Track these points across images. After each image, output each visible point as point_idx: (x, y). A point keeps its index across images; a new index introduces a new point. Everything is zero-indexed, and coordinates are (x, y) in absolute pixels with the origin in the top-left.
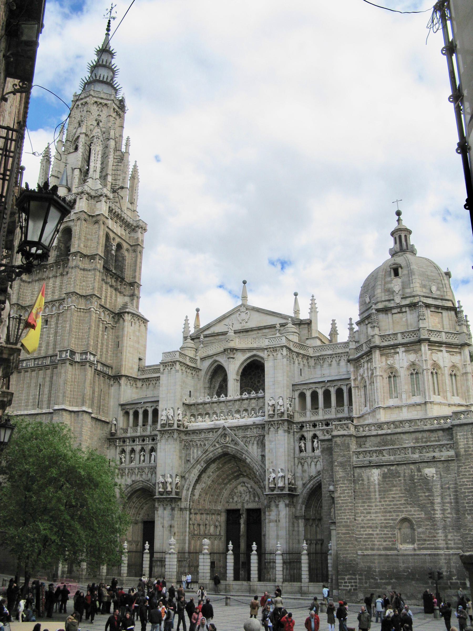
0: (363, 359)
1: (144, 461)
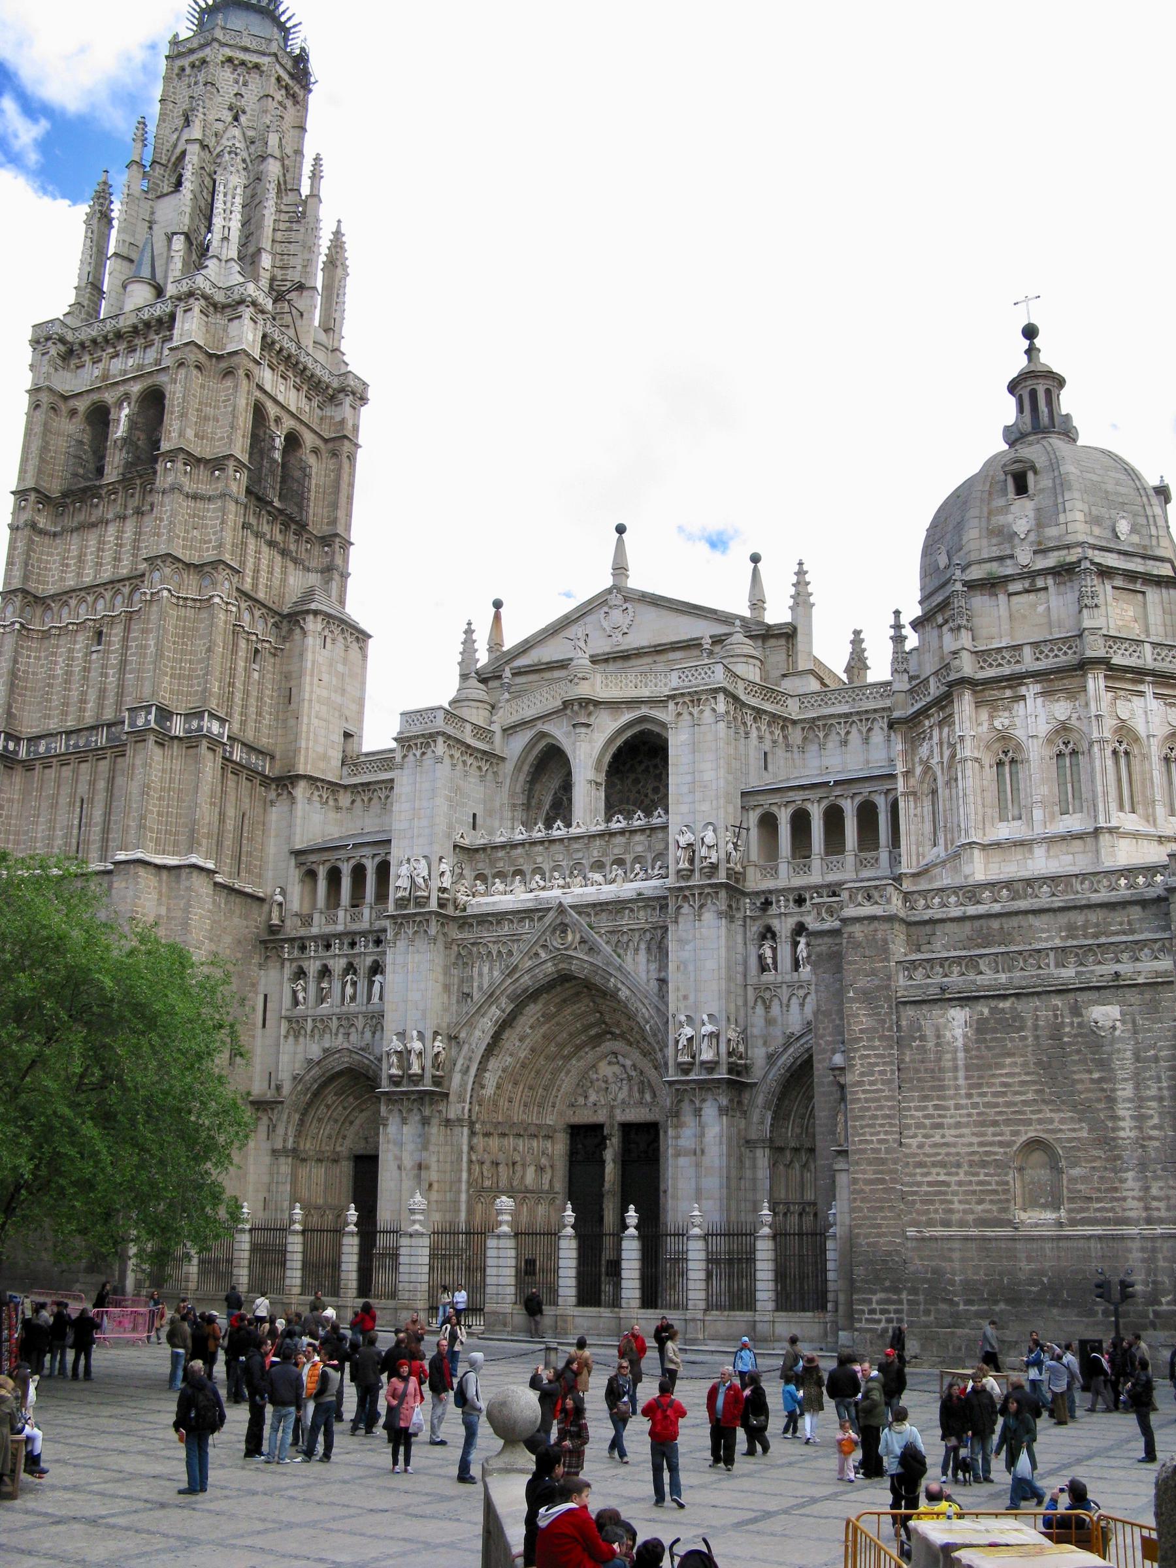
0: (928, 717)
1: (353, 998)
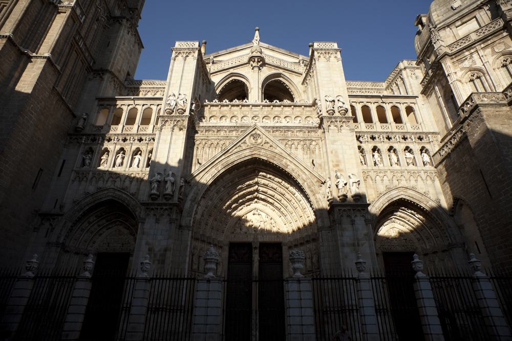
1: (122, 164)
